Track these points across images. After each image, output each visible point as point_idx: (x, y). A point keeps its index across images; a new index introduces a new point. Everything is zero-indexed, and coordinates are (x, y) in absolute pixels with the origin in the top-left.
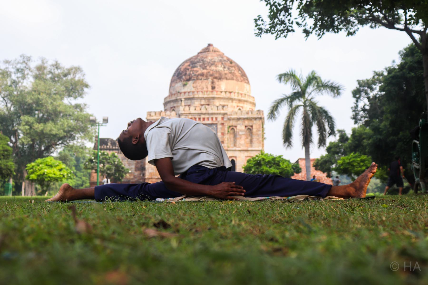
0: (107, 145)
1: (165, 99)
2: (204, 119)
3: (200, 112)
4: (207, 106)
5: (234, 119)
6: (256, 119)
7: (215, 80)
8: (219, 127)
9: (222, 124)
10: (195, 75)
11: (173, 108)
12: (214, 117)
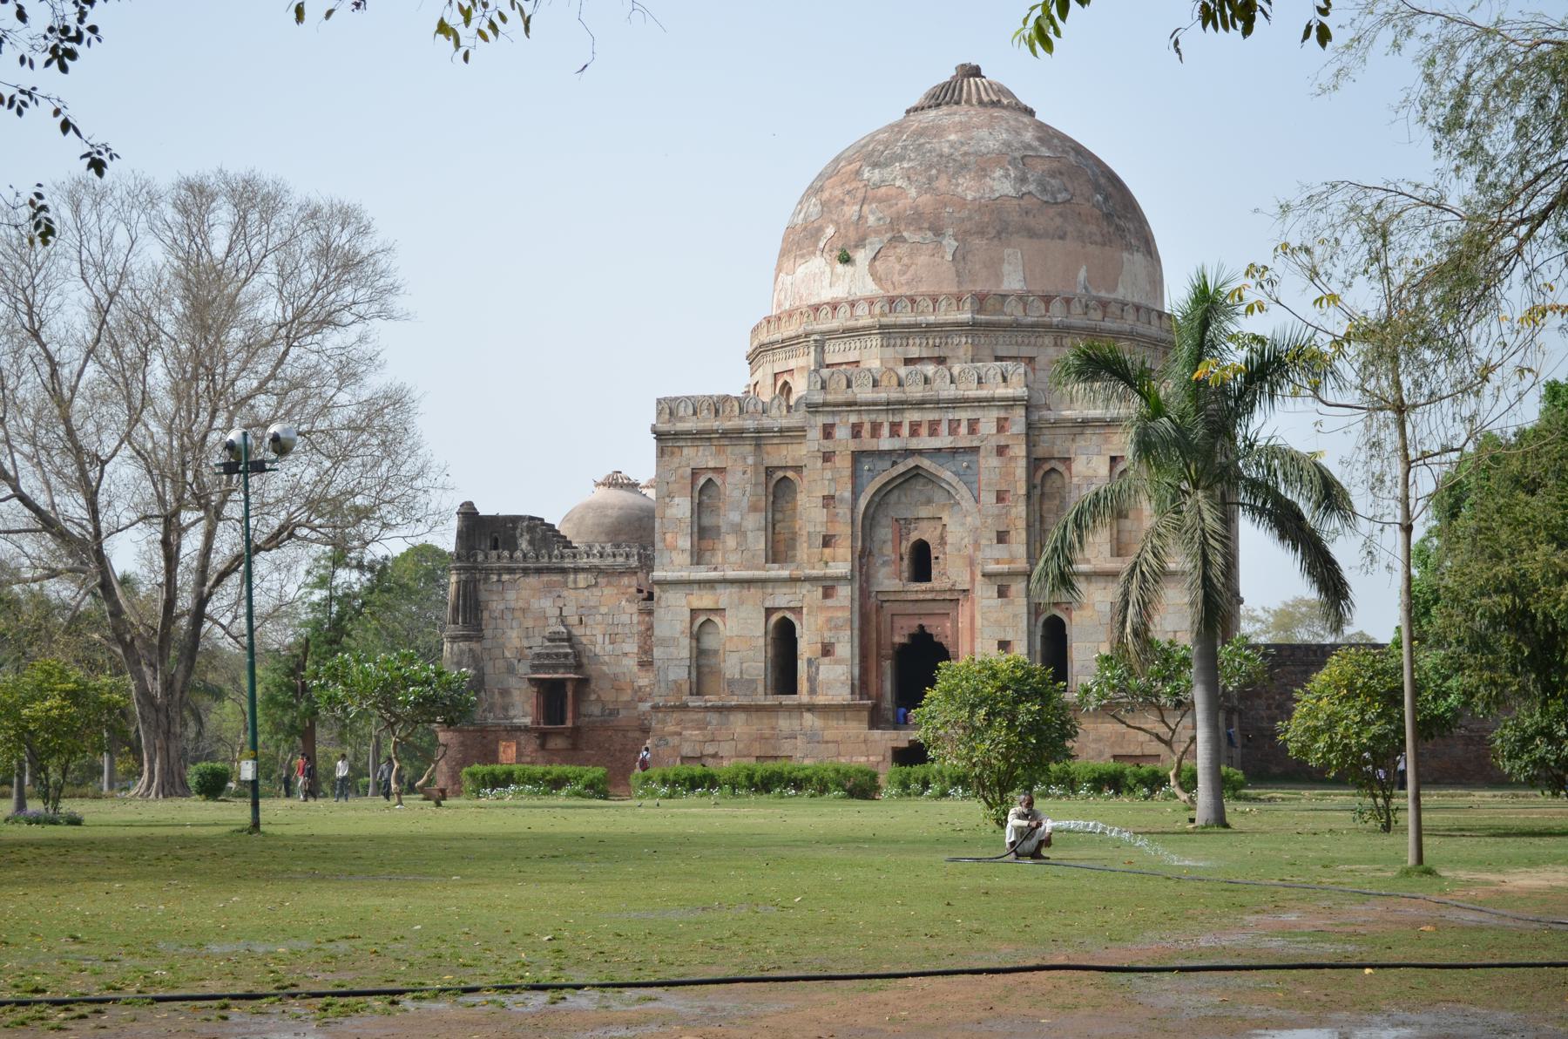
0: (512, 546)
1: (755, 330)
3: (895, 395)
4: (930, 369)
5: (1057, 424)
7: (977, 242)
8: (989, 463)
9: (1001, 450)
11: (786, 377)
12: (964, 415)
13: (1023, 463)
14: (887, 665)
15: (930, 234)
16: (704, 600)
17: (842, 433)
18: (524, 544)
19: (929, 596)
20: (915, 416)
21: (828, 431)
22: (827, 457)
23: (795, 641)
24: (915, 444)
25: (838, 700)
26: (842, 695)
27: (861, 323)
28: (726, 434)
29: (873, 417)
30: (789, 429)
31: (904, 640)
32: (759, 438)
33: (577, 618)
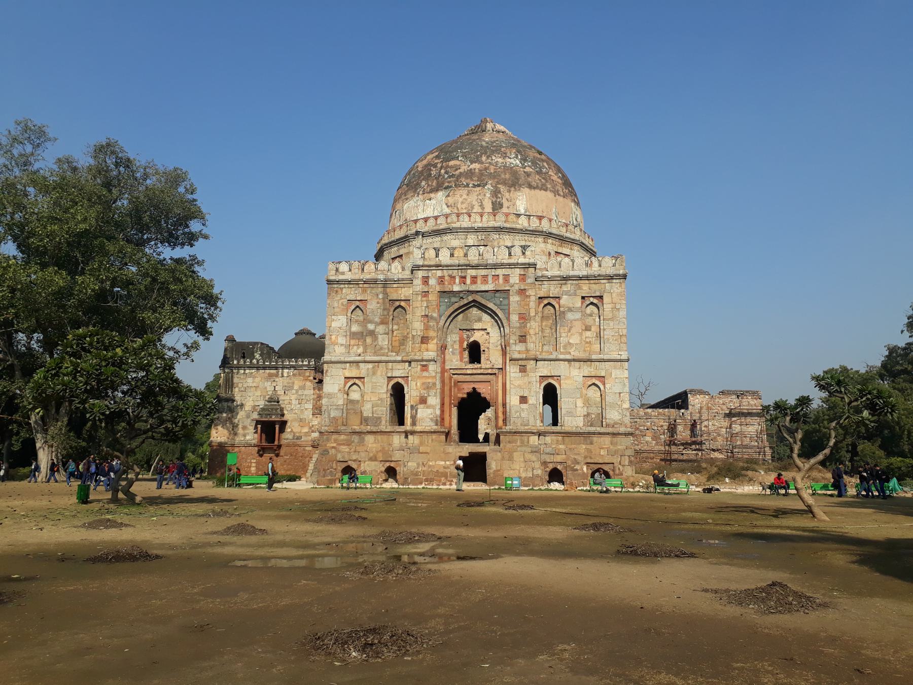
2: (474, 279)
3: (463, 261)
5: (550, 279)
6: (610, 278)
7: (502, 188)
8: (514, 299)
9: (522, 292)
10: (453, 176)
12: (499, 272)
13: (533, 298)
14: (455, 411)
16: (354, 373)
17: (432, 282)
18: (257, 356)
19: (479, 371)
20: (473, 272)
21: (426, 280)
22: (426, 294)
24: (473, 288)
25: (428, 429)
26: (429, 425)
27: (441, 227)
28: (365, 282)
29: (450, 272)
30: (403, 280)
31: (465, 396)
32: (386, 283)
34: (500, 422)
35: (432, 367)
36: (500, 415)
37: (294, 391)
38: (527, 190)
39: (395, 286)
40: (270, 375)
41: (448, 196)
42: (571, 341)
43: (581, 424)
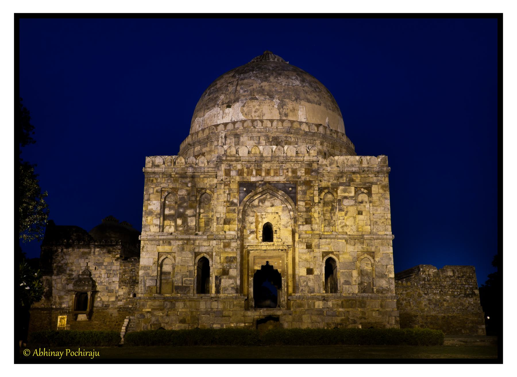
13: (317, 188)
14: (251, 279)
15: (268, 97)
17: (233, 173)
23: (209, 268)
24: (268, 179)
31: (259, 269)
33: (94, 267)
34: (291, 290)
35: (234, 245)
36: (290, 284)
37: (103, 267)
38: (307, 104)
39: (202, 176)
40: (84, 254)
41: (244, 106)
42: (348, 223)
43: (357, 292)
